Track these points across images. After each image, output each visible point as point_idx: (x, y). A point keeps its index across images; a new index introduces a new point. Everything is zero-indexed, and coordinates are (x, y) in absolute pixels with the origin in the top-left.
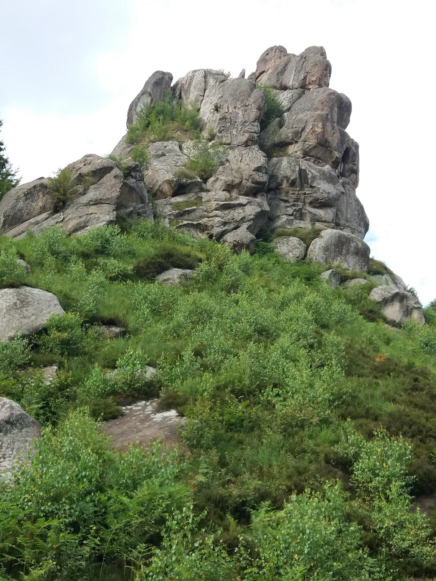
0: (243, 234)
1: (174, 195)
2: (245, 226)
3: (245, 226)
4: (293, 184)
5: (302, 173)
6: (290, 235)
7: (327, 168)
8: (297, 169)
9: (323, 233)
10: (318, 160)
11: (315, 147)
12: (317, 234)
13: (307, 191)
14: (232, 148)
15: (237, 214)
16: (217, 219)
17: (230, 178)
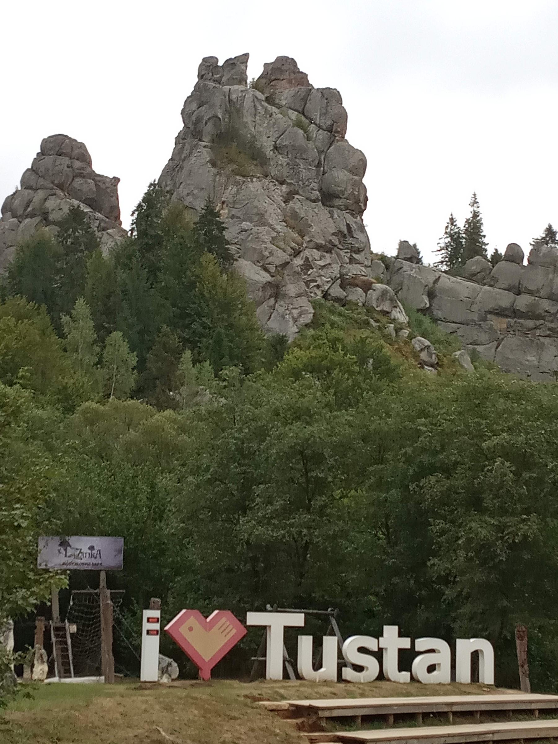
8: (345, 224)
11: (353, 204)
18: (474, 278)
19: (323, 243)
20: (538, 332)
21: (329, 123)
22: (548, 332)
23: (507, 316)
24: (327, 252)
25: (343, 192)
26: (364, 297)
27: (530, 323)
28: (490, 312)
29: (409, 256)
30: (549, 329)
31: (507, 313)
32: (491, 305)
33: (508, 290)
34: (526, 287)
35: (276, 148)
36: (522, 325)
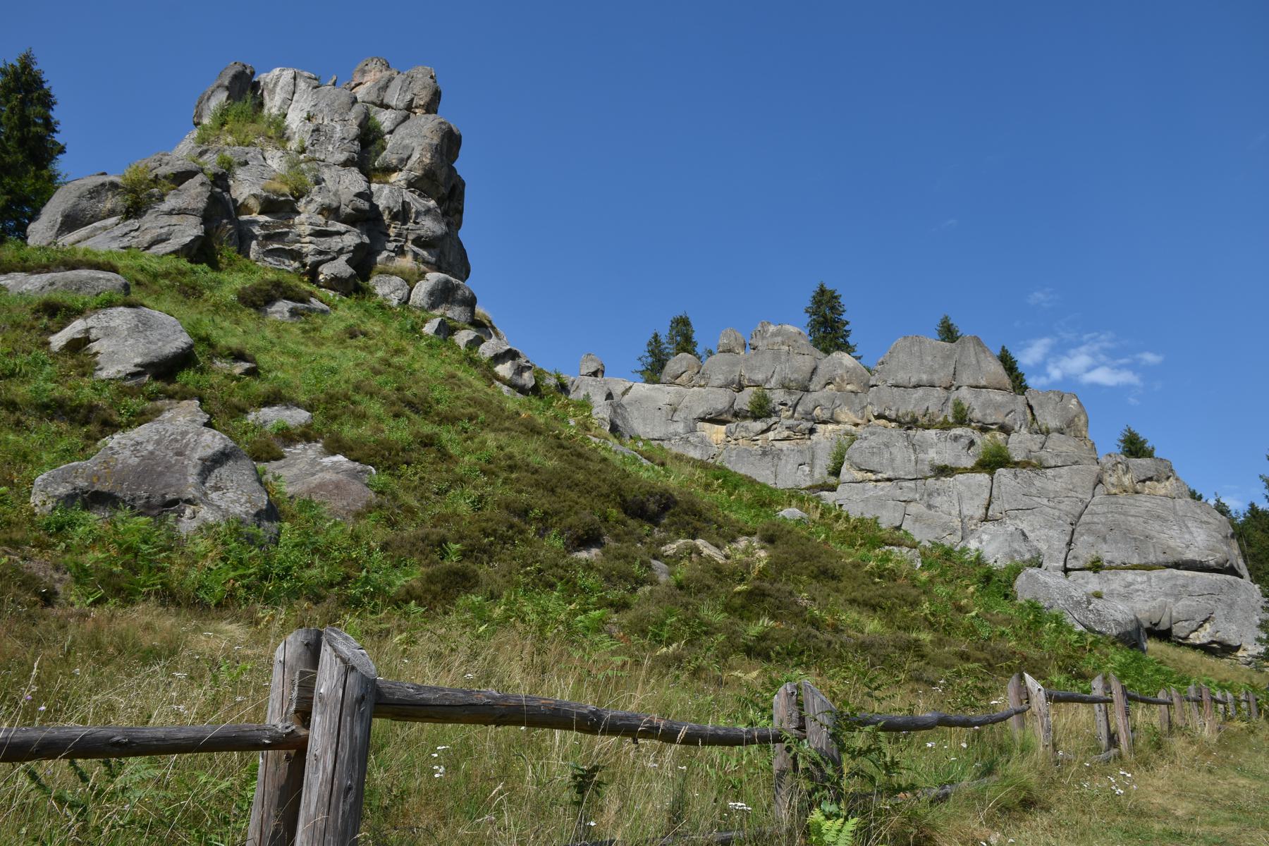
0: (340, 267)
1: (260, 213)
2: (344, 258)
3: (344, 258)
4: (395, 217)
5: (405, 205)
6: (392, 274)
7: (432, 203)
9: (428, 276)
10: (425, 194)
12: (422, 276)
13: (410, 225)
14: (327, 166)
15: (335, 243)
16: (312, 247)
17: (327, 201)
18: (678, 381)
19: (335, 204)
20: (771, 435)
21: (408, 98)
22: (786, 433)
23: (723, 422)
24: (343, 222)
25: (404, 161)
26: (406, 291)
27: (759, 425)
28: (703, 420)
29: (593, 370)
30: (788, 428)
31: (724, 417)
32: (700, 410)
33: (726, 386)
34: (749, 380)
35: (309, 119)
36: (747, 429)
